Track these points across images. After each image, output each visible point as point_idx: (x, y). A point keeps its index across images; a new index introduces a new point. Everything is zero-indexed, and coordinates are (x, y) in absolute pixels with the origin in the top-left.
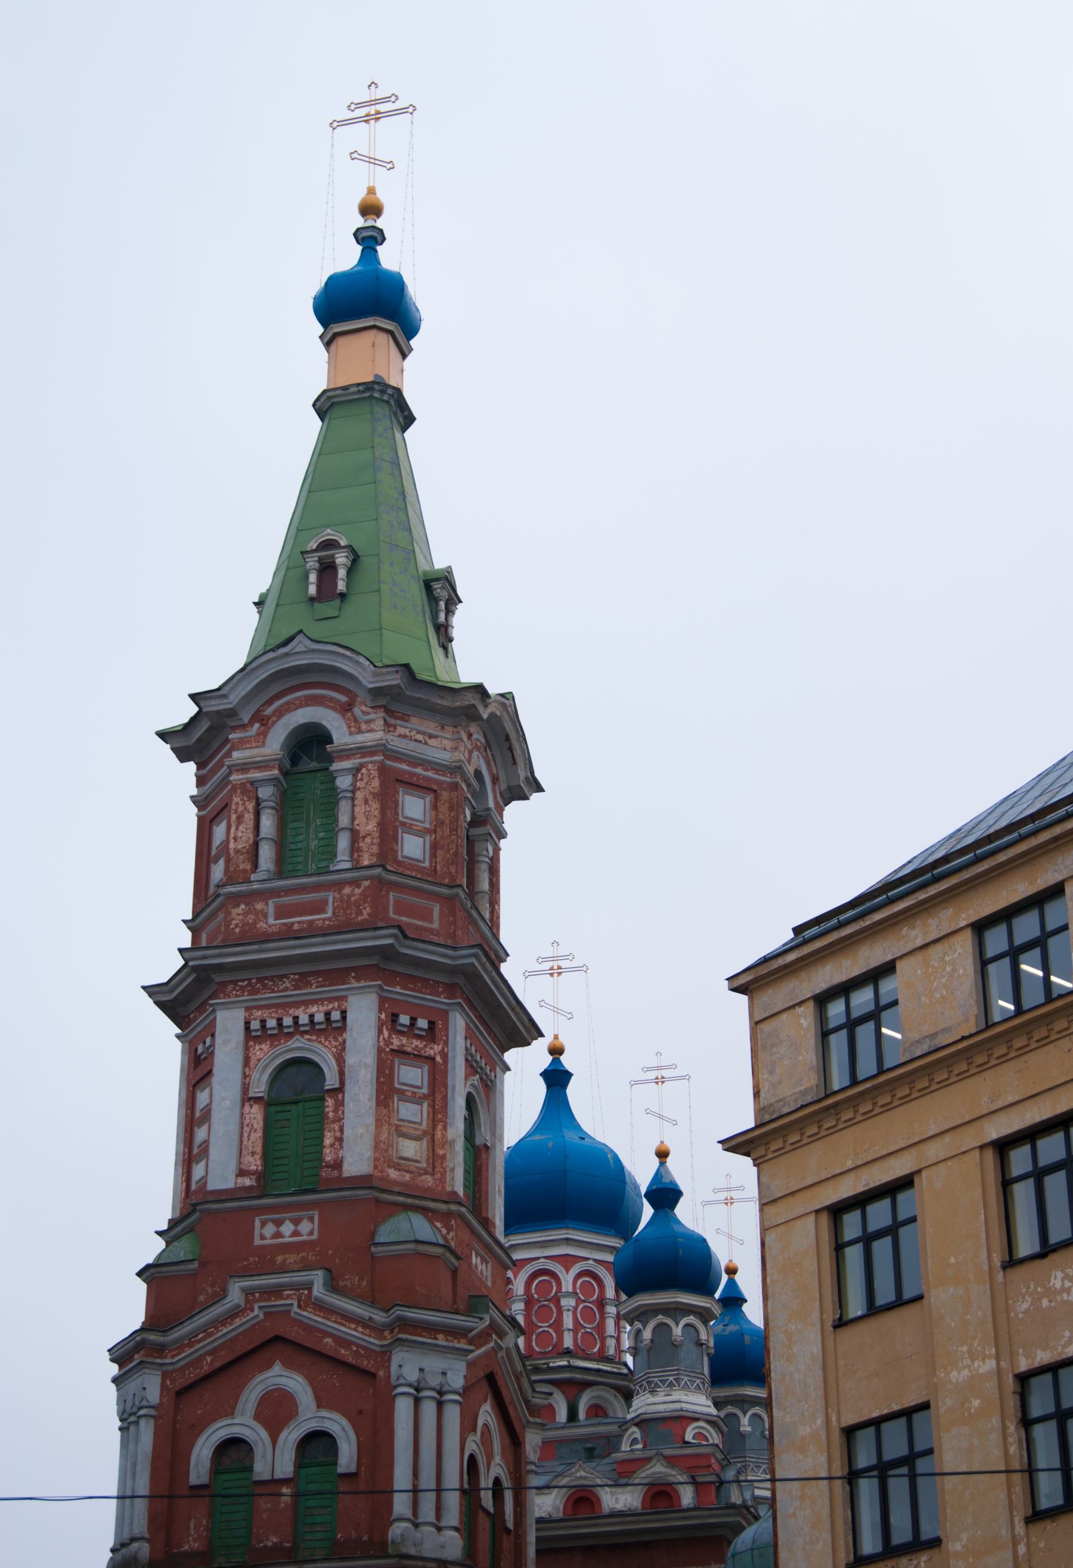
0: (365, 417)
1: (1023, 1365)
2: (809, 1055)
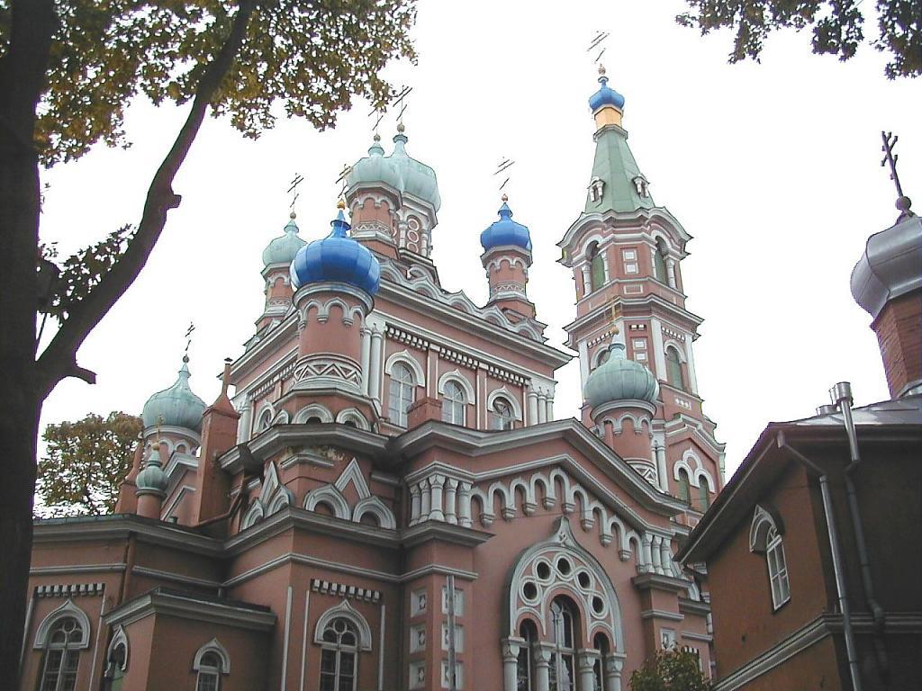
0: (611, 135)
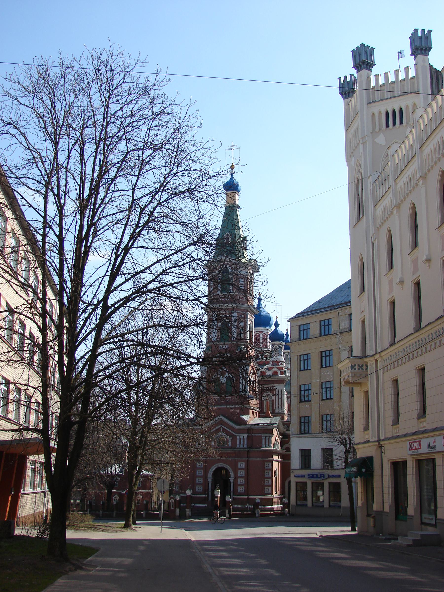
1: (322, 381)
2: (298, 333)
